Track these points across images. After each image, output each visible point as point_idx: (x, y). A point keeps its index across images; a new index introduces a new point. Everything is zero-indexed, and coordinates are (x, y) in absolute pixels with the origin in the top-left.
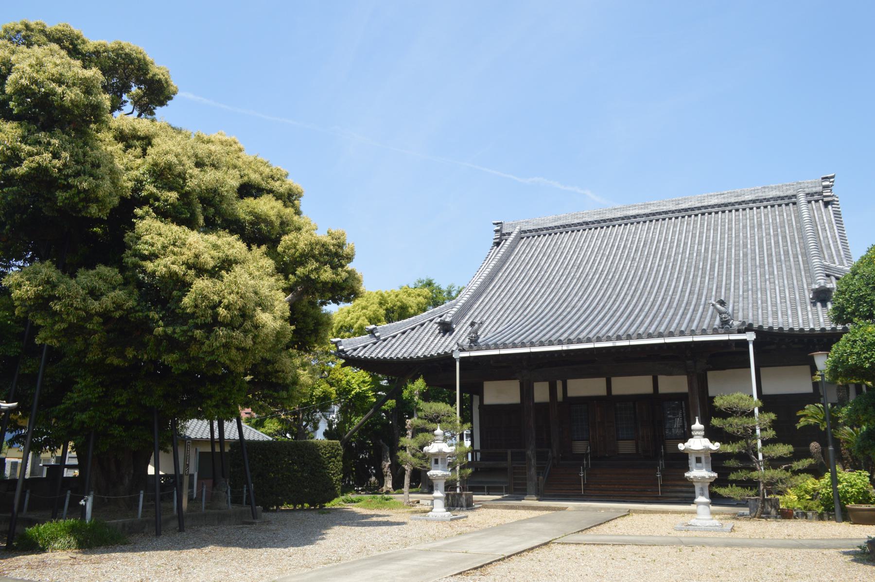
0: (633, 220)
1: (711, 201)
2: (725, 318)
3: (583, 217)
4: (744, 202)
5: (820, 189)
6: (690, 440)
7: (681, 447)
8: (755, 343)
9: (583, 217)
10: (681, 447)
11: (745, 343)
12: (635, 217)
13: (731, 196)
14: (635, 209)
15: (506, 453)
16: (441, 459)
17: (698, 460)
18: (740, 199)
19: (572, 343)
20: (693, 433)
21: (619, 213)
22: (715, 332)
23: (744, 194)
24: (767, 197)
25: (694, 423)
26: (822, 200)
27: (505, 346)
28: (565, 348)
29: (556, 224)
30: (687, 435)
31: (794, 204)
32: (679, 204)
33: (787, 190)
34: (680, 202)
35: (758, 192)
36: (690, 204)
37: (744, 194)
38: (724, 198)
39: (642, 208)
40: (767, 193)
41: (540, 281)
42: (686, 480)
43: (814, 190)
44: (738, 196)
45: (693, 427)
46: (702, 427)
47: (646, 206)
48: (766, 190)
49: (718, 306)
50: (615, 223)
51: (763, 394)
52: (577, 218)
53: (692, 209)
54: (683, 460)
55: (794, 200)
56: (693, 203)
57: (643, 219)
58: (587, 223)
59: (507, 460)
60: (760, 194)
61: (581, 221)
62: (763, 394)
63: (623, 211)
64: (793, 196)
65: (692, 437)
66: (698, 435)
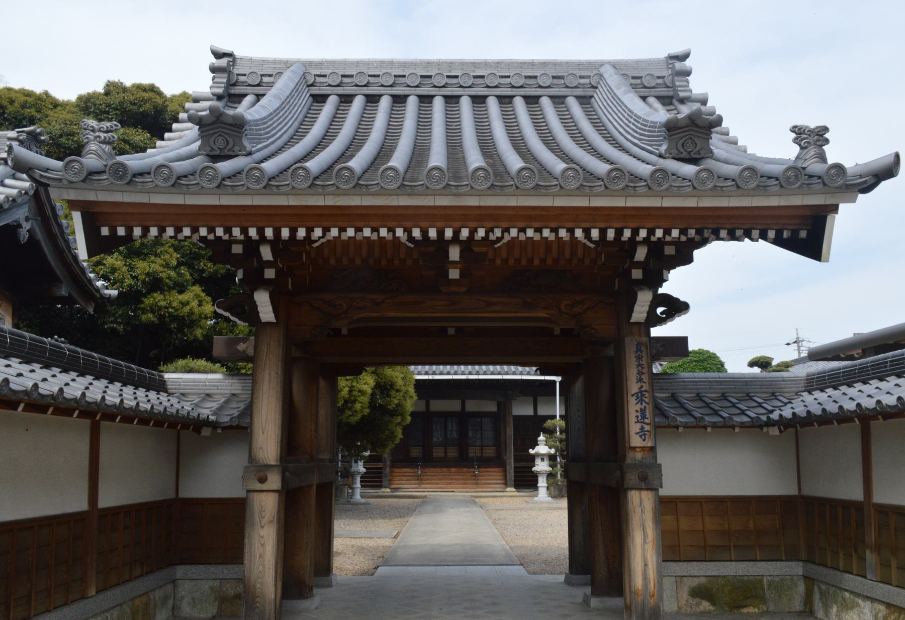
6: (537, 447)
7: (531, 451)
8: (560, 383)
10: (531, 451)
11: (554, 382)
17: (543, 460)
19: (436, 374)
20: (539, 443)
25: (539, 436)
28: (430, 377)
30: (535, 444)
42: (533, 472)
45: (539, 439)
46: (544, 438)
54: (532, 459)
65: (538, 445)
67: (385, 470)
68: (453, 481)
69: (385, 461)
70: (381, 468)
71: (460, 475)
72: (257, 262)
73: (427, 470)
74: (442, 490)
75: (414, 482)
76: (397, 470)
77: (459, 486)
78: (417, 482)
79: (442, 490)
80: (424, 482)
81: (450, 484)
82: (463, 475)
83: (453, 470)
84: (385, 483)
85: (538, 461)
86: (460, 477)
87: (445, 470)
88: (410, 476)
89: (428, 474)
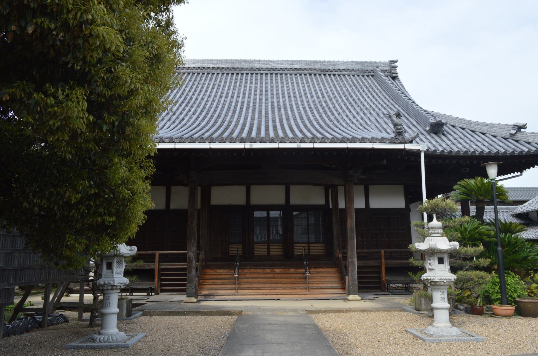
0: (257, 71)
1: (316, 66)
2: (400, 129)
3: (217, 63)
4: (339, 70)
5: (388, 68)
9: (217, 63)
12: (259, 69)
13: (330, 64)
14: (260, 63)
15: (154, 255)
16: (117, 261)
17: (441, 261)
18: (336, 67)
21: (246, 64)
22: (392, 141)
23: (339, 64)
24: (354, 69)
26: (390, 76)
27: (181, 141)
28: (248, 146)
29: (194, 66)
31: (372, 76)
32: (292, 64)
33: (368, 66)
34: (294, 63)
35: (348, 65)
36: (301, 65)
37: (339, 64)
38: (325, 65)
39: (264, 63)
40: (354, 66)
41: (188, 104)
43: (385, 69)
44: (334, 65)
47: (268, 62)
48: (354, 64)
49: (394, 118)
50: (244, 72)
51: (370, 208)
52: (212, 63)
53: (303, 70)
55: (372, 73)
56: (303, 65)
57: (266, 72)
58: (221, 69)
59: (154, 262)
60: (350, 66)
61: (216, 66)
62: (370, 208)
63: (250, 63)
64: (372, 70)
66: (438, 233)
67: (190, 272)
68: (278, 285)
69: (190, 261)
70: (185, 269)
71: (287, 278)
72: (85, 70)
73: (246, 271)
74: (264, 297)
75: (230, 286)
76: (210, 271)
77: (286, 291)
78: (234, 286)
79: (264, 297)
80: (242, 286)
81: (275, 288)
82: (291, 277)
83: (278, 270)
84: (190, 287)
85: (432, 264)
86: (286, 280)
87: (268, 270)
88: (225, 279)
89: (247, 276)
